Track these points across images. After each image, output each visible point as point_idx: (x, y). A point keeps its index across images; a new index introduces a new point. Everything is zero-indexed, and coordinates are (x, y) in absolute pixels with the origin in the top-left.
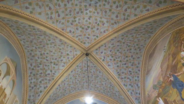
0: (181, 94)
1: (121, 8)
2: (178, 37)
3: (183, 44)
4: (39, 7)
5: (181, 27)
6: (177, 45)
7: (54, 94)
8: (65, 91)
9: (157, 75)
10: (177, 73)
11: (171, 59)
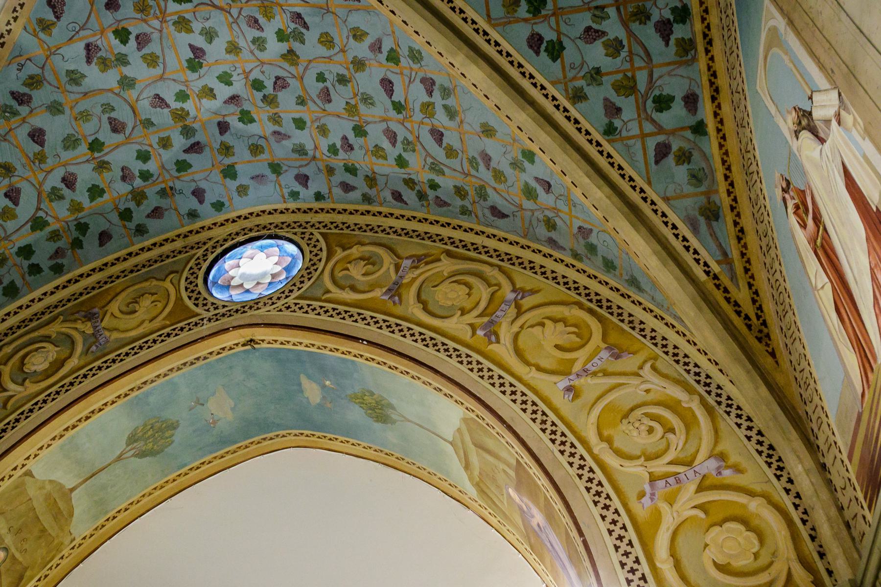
1: (47, 187)
4: (493, 164)
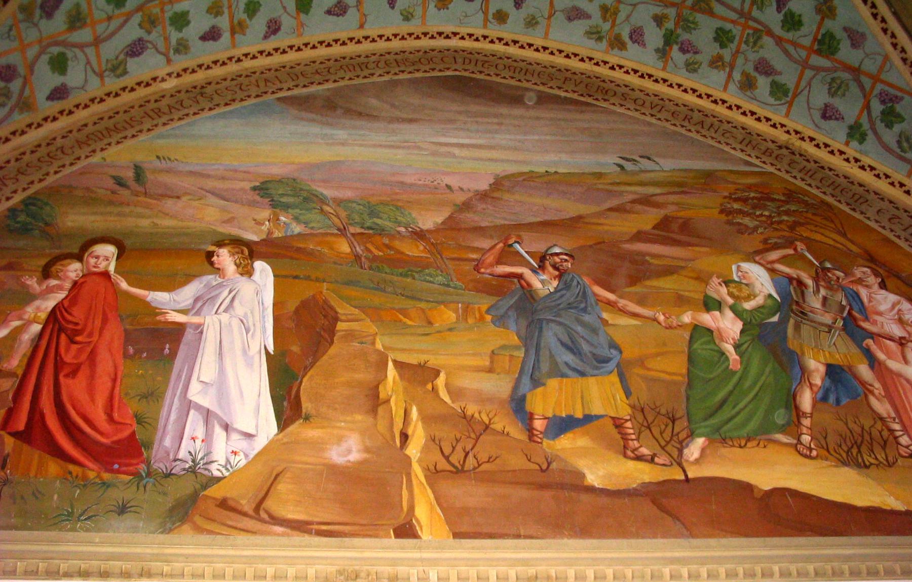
0: (536, 383)
2: (787, 213)
3: (795, 249)
5: (844, 207)
6: (747, 221)
9: (408, 180)
10: (621, 297)
11: (647, 220)
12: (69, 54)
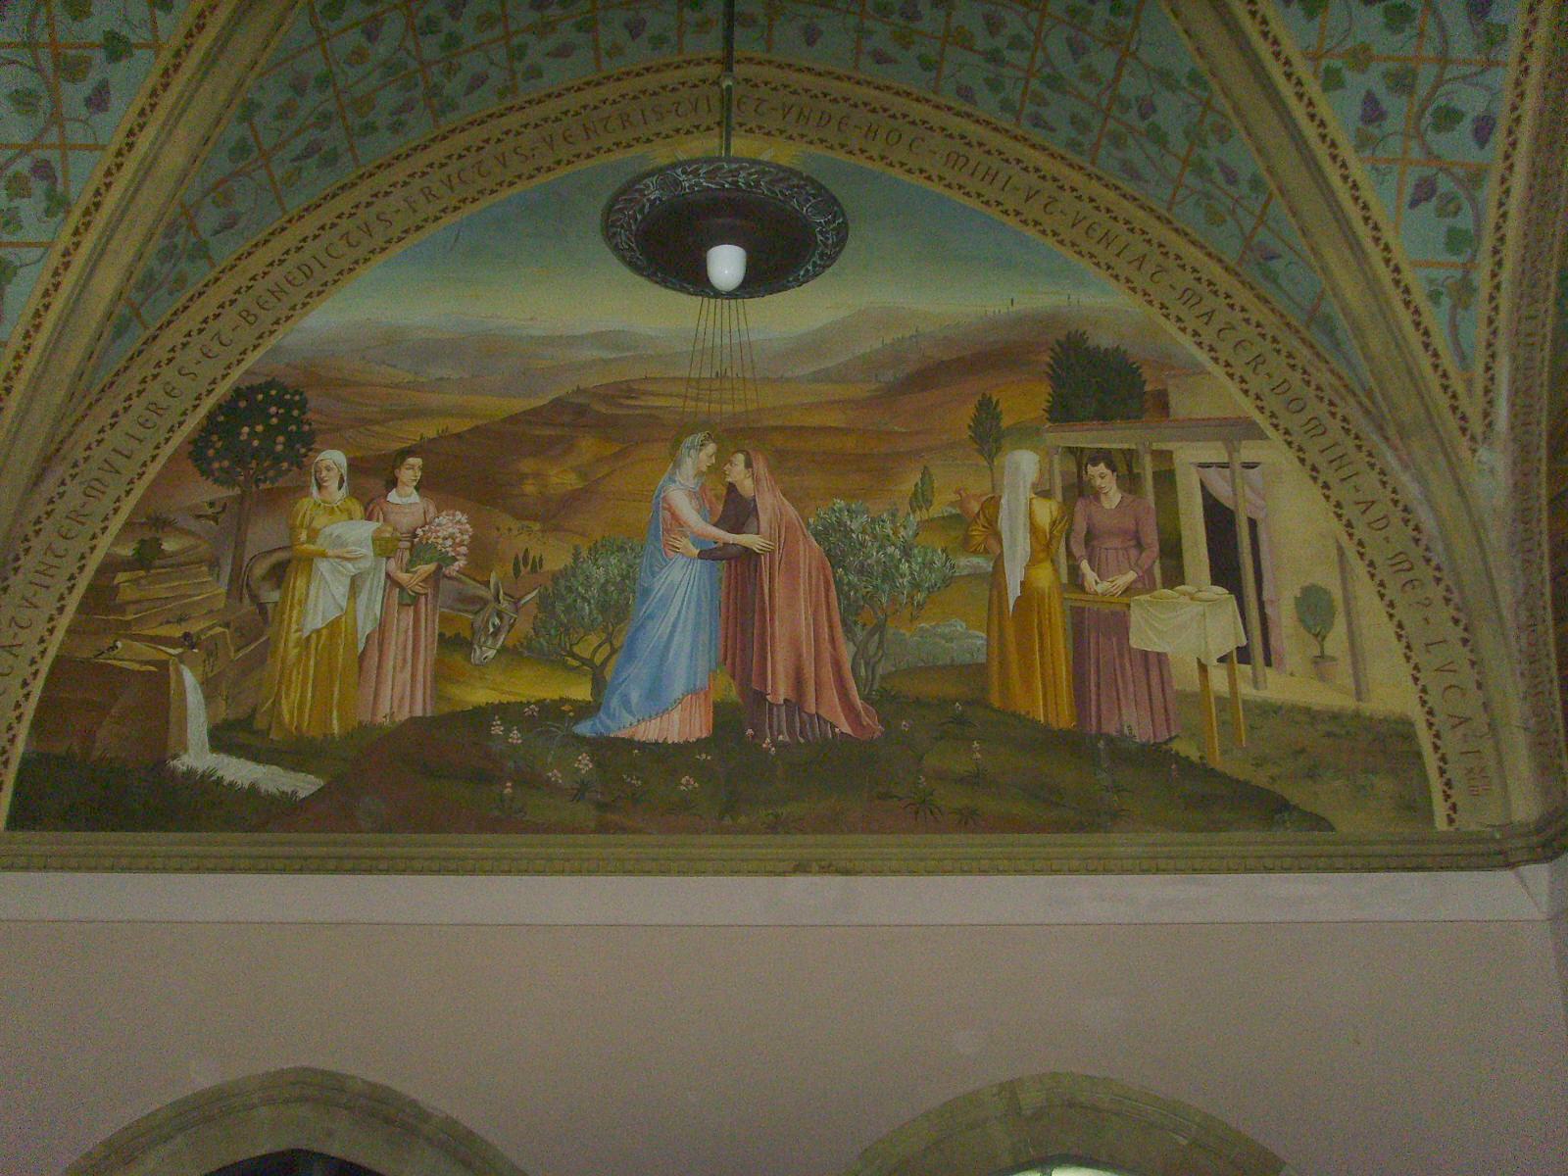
7: (299, 87)
8: (453, 41)
12: (1442, 102)
